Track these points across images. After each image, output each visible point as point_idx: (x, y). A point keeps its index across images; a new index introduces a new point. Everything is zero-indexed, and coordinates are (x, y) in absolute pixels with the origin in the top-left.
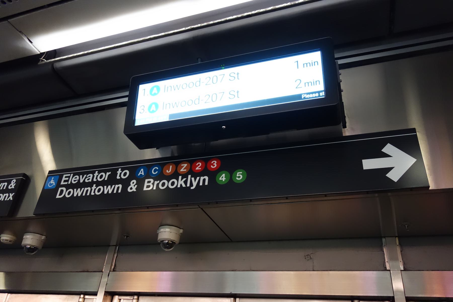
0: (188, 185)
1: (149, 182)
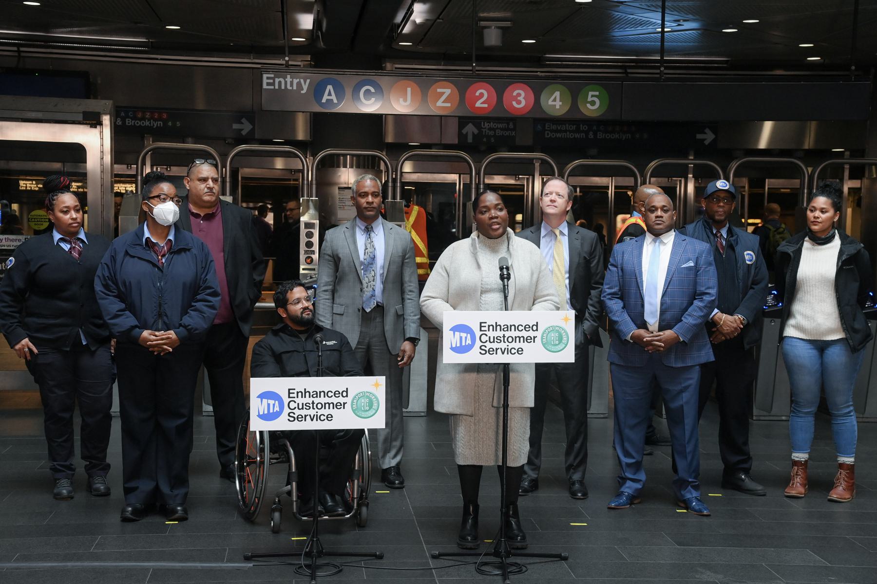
0: (621, 137)
1: (600, 134)
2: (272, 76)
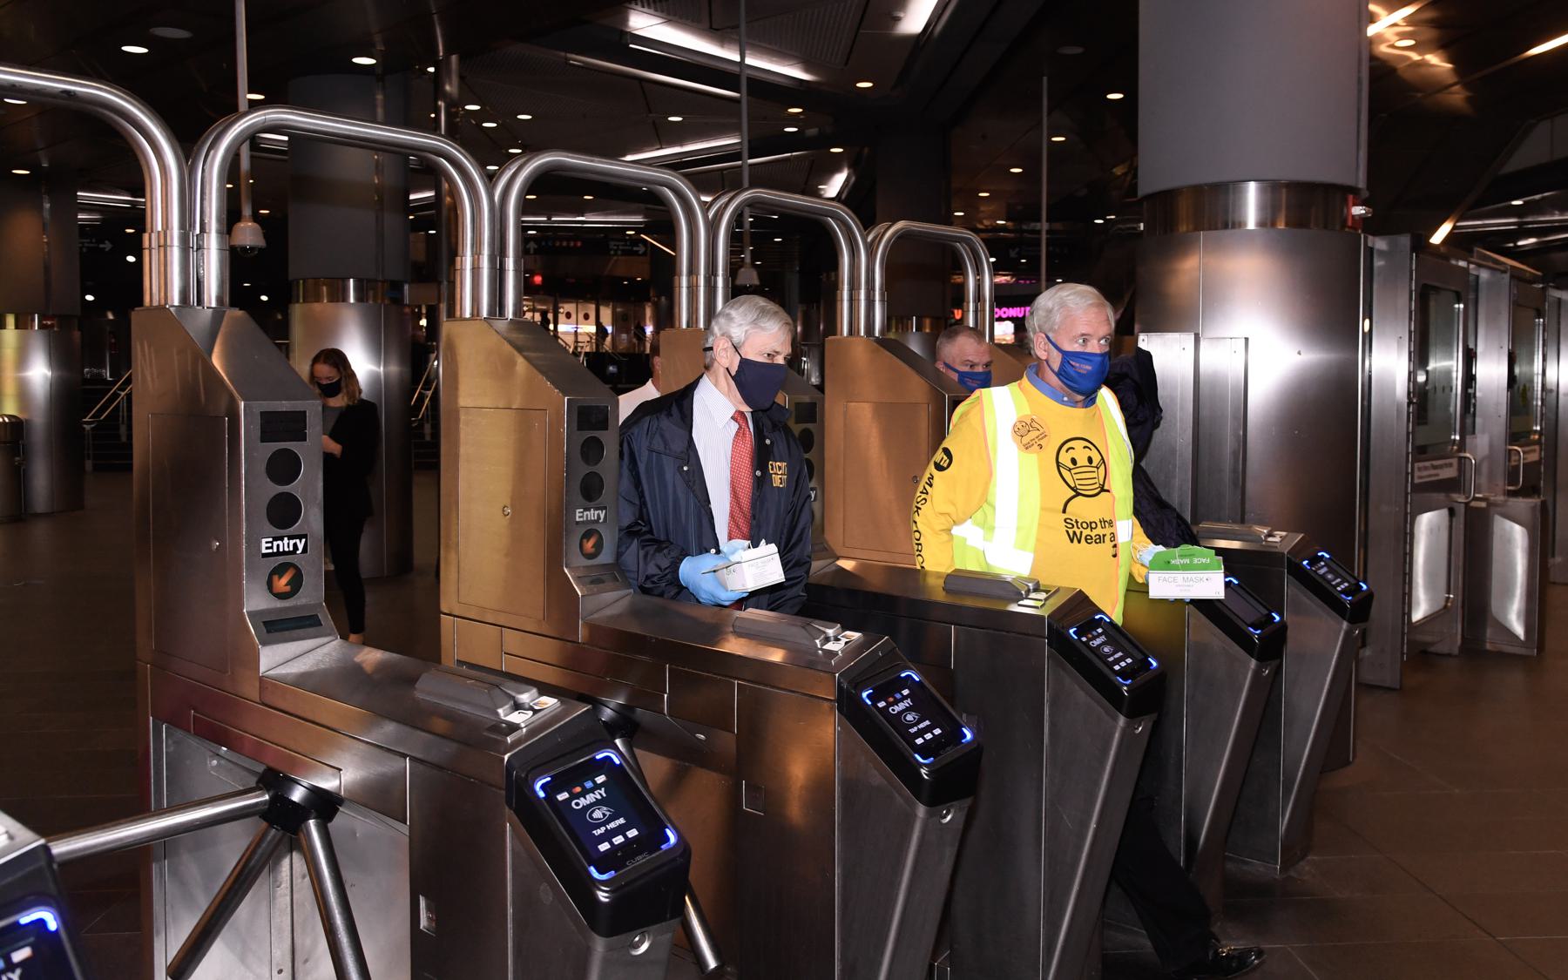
2: (271, 539)
